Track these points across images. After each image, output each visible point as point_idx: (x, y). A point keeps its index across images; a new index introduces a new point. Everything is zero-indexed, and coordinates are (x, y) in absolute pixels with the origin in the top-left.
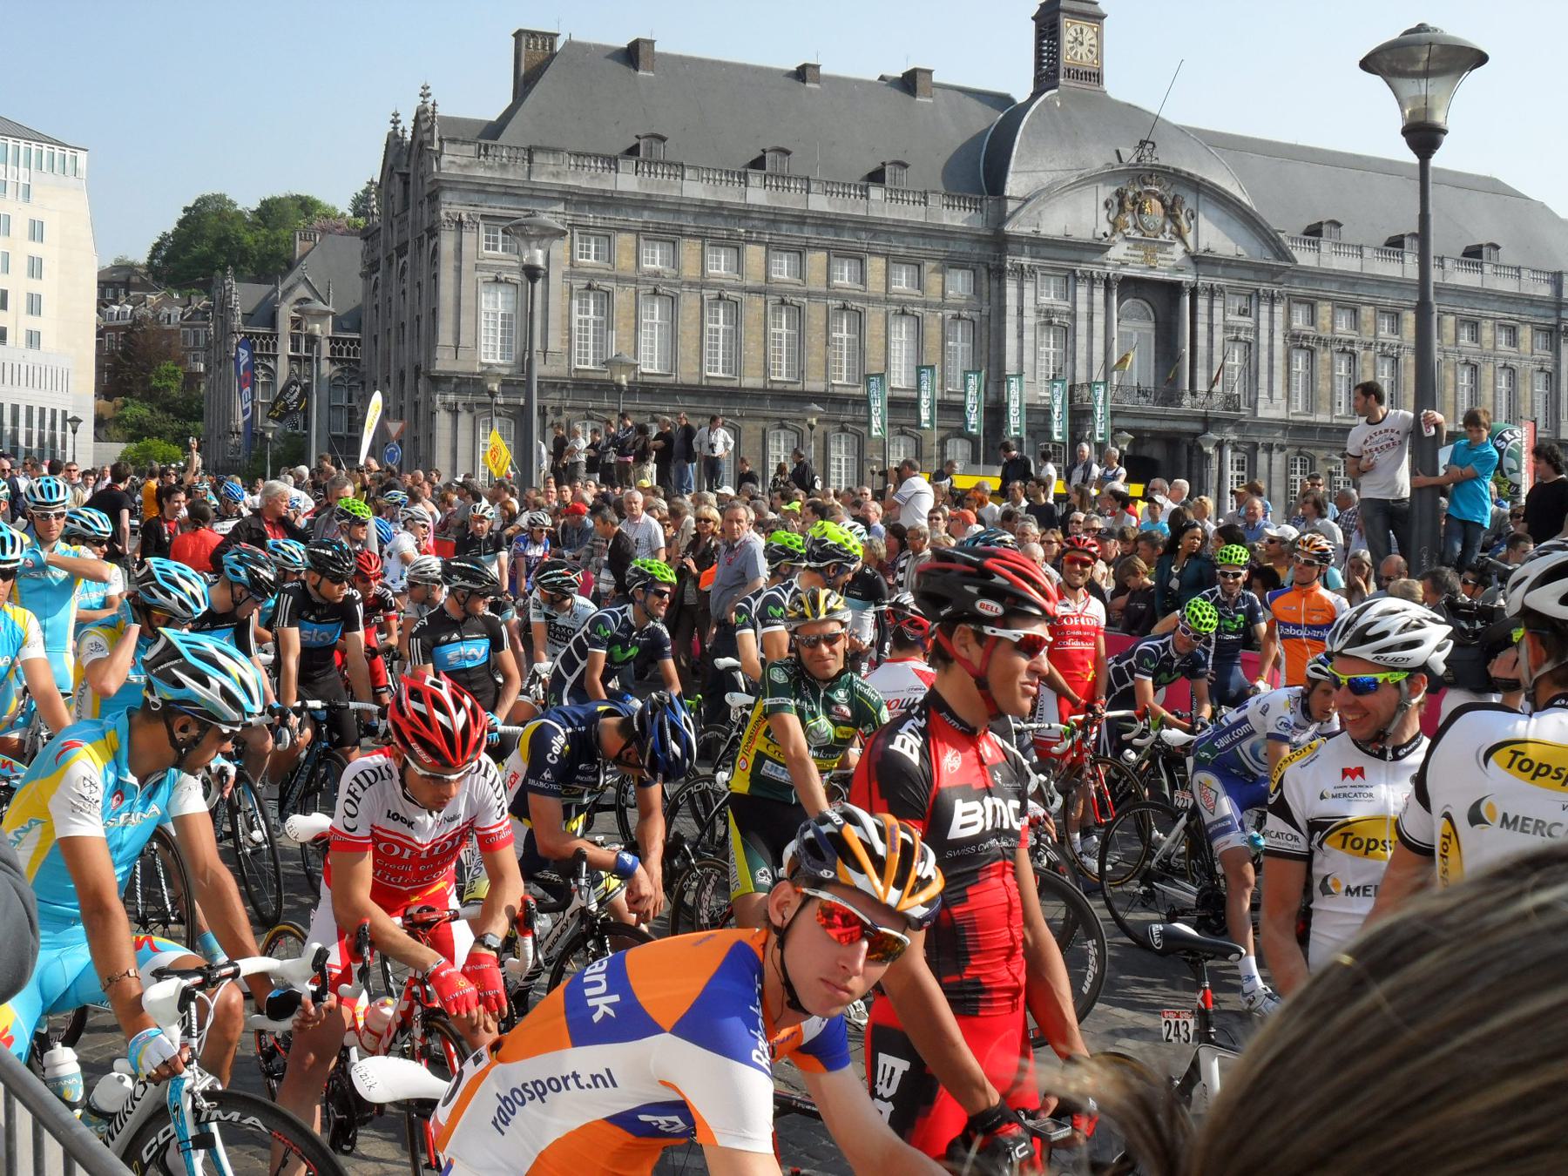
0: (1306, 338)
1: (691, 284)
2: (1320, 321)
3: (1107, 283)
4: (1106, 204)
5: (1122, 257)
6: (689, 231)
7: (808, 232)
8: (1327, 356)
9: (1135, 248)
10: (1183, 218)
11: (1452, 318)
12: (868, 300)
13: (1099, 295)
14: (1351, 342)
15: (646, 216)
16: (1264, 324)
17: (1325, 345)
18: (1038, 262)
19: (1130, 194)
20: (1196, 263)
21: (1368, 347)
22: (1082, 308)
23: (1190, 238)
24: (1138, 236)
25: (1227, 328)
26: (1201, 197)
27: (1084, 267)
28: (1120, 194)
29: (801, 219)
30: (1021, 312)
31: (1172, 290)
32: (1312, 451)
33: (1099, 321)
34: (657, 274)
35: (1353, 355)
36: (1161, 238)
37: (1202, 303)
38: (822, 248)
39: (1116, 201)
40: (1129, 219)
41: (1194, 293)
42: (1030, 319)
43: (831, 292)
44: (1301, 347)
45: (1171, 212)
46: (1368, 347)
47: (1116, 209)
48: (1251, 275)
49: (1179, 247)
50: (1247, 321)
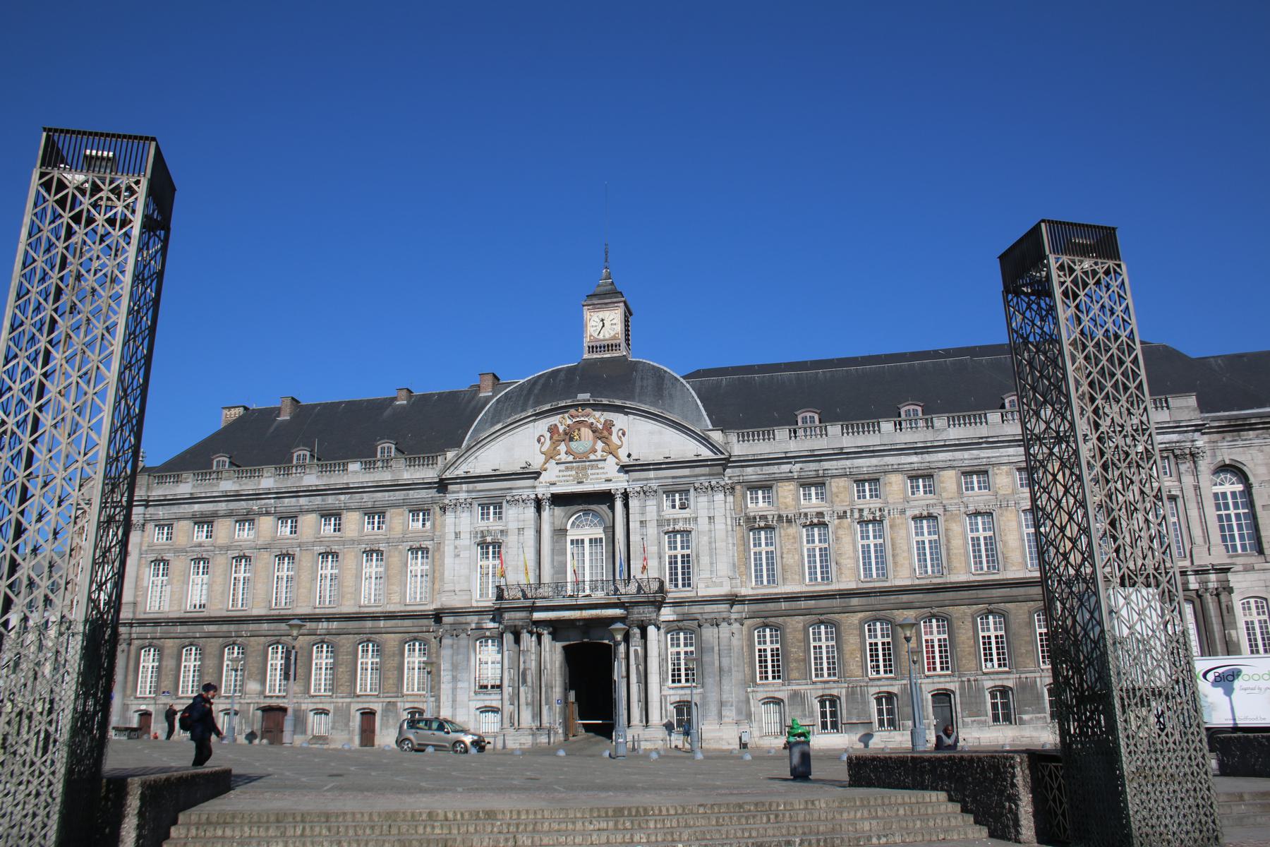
0: (764, 517)
1: (221, 548)
2: (781, 500)
3: (538, 504)
4: (539, 441)
5: (557, 479)
6: (221, 513)
7: (303, 501)
8: (792, 530)
9: (567, 468)
10: (614, 438)
11: (952, 473)
12: (344, 543)
13: (531, 511)
14: (820, 514)
15: (196, 507)
16: (703, 515)
17: (789, 521)
18: (474, 495)
19: (561, 429)
20: (627, 472)
21: (842, 516)
22: (512, 526)
23: (622, 454)
24: (570, 458)
25: (660, 523)
26: (631, 417)
27: (515, 492)
28: (553, 429)
29: (296, 494)
30: (457, 535)
31: (606, 498)
32: (780, 620)
33: (530, 534)
34: (200, 545)
35: (825, 525)
36: (592, 457)
37: (633, 503)
38: (313, 511)
39: (548, 435)
40: (562, 448)
41: (626, 496)
42: (466, 540)
43: (319, 541)
44: (760, 528)
45: (602, 434)
46: (842, 516)
47: (548, 443)
48: (686, 472)
49: (611, 460)
50: (685, 513)
